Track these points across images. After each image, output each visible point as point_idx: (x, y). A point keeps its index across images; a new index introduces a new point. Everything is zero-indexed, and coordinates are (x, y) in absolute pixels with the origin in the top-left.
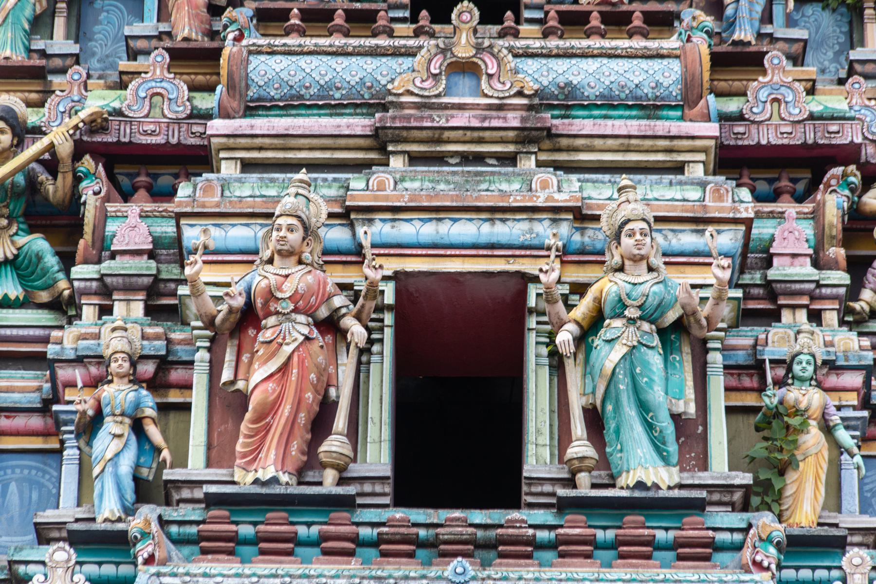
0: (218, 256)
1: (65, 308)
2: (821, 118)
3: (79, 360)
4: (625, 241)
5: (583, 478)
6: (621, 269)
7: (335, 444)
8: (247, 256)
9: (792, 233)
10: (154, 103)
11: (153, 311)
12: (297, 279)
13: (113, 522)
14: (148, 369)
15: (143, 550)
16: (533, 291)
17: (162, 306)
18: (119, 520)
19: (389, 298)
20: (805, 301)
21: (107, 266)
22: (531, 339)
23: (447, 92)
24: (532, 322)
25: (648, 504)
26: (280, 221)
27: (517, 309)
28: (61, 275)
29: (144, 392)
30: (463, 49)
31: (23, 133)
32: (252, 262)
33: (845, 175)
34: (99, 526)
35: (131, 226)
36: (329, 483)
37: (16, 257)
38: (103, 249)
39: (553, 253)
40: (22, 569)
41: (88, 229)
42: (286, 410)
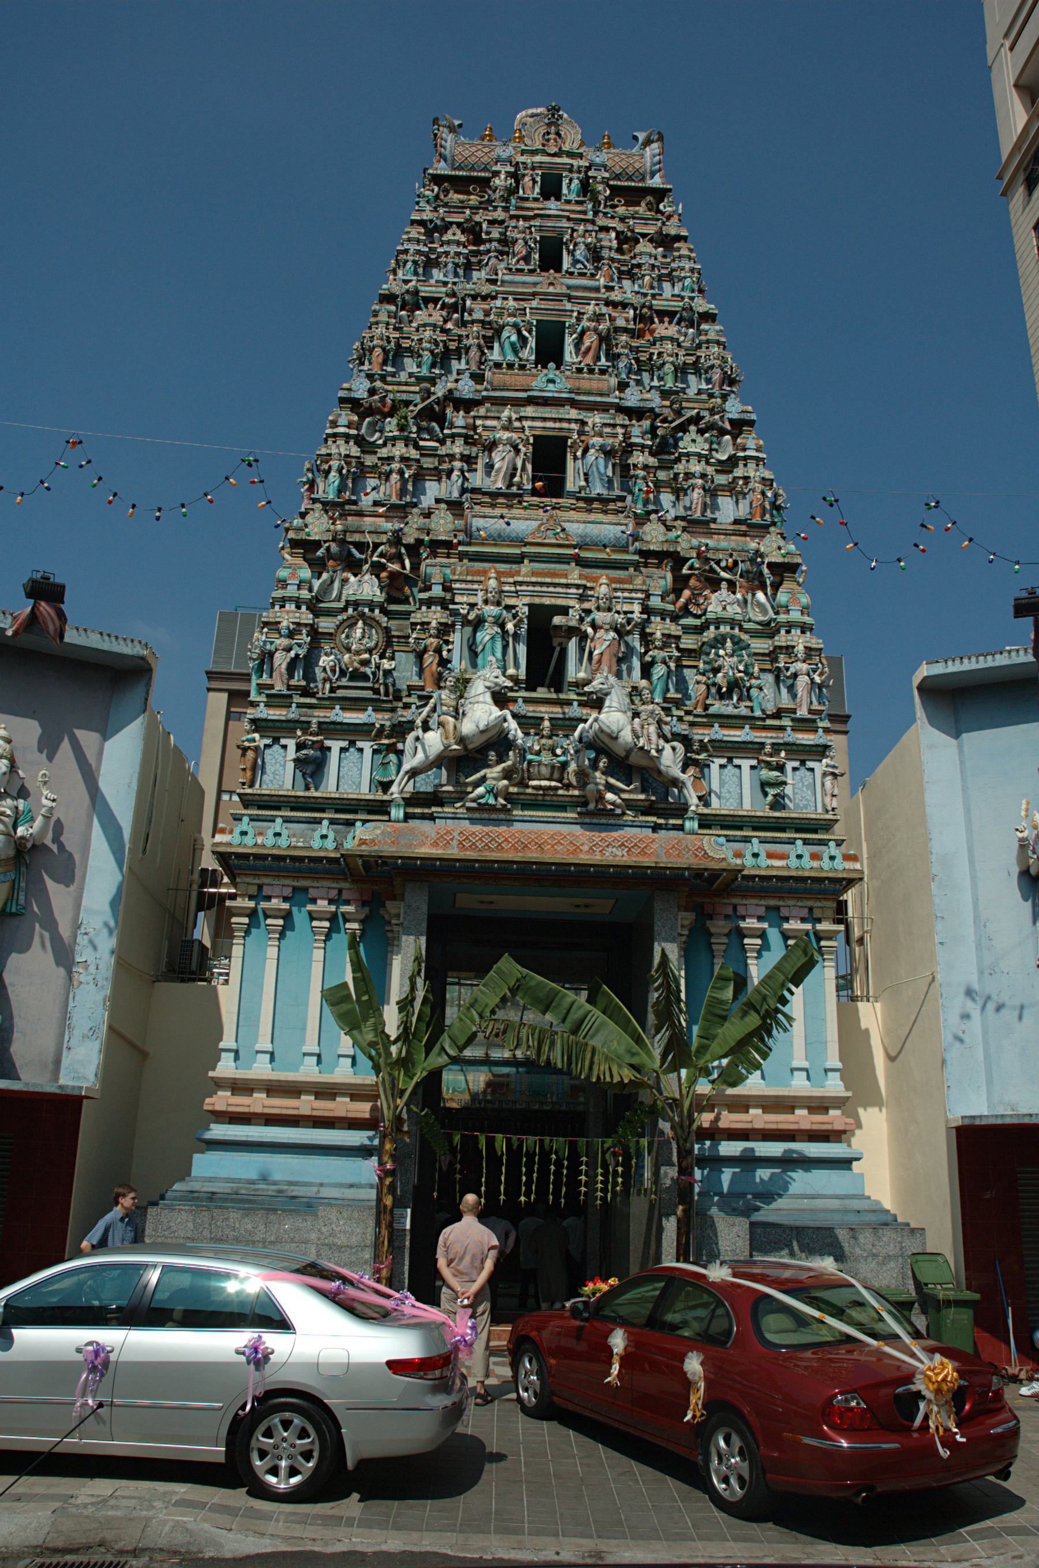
0: (485, 428)
1: (442, 442)
3: (447, 455)
7: (517, 479)
8: (493, 429)
9: (638, 431)
10: (466, 388)
11: (466, 443)
12: (506, 435)
15: (466, 505)
16: (570, 442)
17: (468, 441)
19: (531, 440)
25: (600, 499)
27: (565, 446)
30: (551, 376)
31: (429, 394)
35: (460, 419)
36: (514, 489)
38: (452, 426)
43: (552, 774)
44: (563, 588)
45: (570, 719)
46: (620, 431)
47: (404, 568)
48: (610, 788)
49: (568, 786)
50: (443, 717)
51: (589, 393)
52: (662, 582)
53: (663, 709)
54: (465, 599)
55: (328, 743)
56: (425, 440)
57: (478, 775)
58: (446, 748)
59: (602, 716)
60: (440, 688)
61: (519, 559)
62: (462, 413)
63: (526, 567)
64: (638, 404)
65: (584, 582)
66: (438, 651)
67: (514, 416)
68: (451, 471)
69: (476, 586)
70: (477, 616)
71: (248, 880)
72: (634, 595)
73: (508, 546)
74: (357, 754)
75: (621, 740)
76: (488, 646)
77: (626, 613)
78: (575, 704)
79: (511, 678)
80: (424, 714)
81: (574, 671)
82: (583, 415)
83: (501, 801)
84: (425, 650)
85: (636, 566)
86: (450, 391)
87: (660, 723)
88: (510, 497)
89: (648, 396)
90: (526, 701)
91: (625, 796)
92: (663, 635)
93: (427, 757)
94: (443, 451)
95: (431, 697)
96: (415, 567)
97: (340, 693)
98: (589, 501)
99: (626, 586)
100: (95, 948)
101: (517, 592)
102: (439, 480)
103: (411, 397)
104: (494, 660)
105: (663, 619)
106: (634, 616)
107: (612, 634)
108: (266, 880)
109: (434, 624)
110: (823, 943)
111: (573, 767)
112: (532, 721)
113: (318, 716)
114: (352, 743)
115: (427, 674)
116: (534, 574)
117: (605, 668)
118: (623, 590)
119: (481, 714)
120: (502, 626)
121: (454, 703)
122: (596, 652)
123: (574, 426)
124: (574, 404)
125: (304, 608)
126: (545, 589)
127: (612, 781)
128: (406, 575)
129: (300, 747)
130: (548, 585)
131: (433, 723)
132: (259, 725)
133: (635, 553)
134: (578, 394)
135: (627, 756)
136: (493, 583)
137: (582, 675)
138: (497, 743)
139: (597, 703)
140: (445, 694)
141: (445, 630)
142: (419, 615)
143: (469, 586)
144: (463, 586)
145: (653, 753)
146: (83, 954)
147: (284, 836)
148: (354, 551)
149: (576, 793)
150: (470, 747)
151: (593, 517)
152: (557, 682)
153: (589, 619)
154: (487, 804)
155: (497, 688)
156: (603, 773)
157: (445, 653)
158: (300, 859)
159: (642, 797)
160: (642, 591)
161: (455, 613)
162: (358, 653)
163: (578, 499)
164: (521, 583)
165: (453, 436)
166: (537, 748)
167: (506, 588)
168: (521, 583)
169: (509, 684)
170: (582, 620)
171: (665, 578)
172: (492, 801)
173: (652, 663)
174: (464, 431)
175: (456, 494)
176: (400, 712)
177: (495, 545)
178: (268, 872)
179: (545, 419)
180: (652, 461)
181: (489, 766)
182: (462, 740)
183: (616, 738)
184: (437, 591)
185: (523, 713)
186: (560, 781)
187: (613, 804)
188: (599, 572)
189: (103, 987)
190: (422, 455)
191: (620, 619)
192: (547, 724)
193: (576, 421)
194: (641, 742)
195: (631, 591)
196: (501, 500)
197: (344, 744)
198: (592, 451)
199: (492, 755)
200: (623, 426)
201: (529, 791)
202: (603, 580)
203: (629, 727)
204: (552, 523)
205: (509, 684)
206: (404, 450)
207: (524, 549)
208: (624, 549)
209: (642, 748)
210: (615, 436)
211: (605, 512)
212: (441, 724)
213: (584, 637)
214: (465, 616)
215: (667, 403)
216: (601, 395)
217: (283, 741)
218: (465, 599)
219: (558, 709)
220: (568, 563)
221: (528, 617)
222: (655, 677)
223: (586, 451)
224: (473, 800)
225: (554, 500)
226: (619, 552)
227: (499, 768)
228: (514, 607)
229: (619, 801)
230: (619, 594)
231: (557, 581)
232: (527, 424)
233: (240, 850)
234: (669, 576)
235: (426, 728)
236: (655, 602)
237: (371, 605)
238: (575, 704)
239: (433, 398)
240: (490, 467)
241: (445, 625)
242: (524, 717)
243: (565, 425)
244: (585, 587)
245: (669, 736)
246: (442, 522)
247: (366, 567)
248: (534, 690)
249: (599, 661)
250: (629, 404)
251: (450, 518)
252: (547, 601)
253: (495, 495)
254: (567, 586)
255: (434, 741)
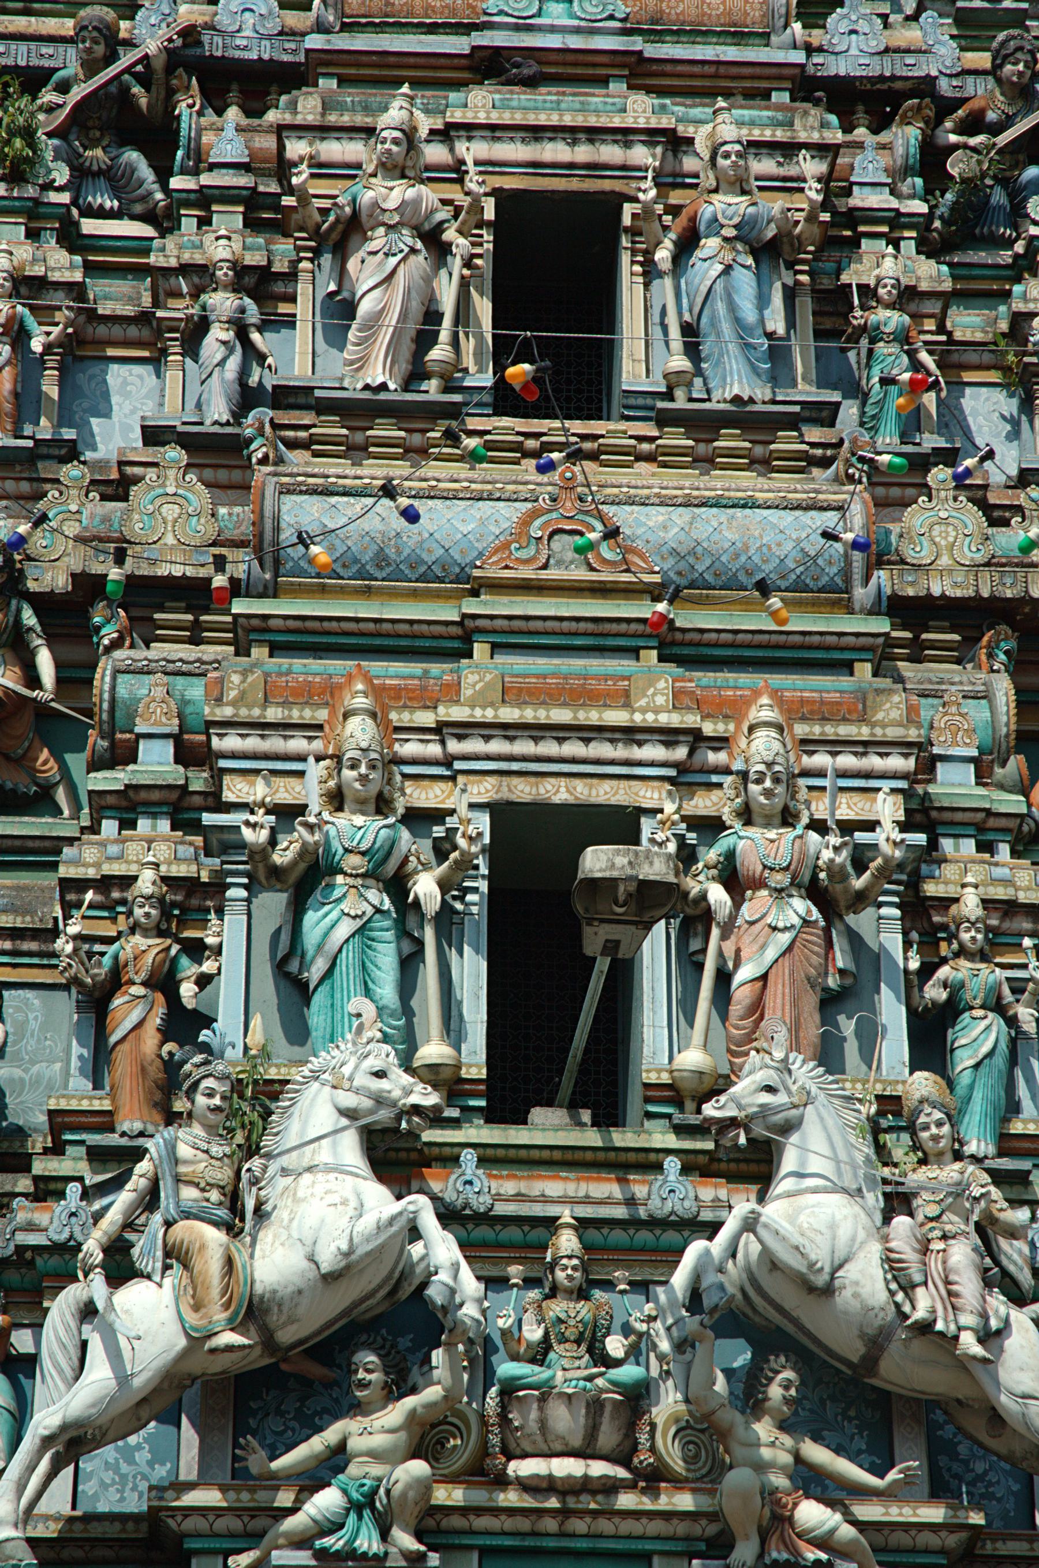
0: (322, 169)
2: (897, 50)
3: (184, 269)
4: (721, 162)
5: (680, 393)
6: (716, 191)
11: (252, 224)
12: (396, 194)
13: (221, 425)
14: (249, 280)
16: (628, 210)
17: (261, 215)
18: (228, 423)
19: (489, 214)
20: (885, 229)
21: (206, 179)
22: (625, 258)
23: (539, 14)
24: (625, 242)
25: (742, 417)
26: (384, 134)
28: (156, 186)
29: (247, 301)
31: (114, 45)
32: (354, 177)
33: (919, 108)
34: (208, 428)
35: (227, 138)
37: (110, 168)
38: (199, 162)
39: (650, 174)
40: (129, 470)
41: (183, 141)
42: (393, 318)
43: (592, 1432)
44: (611, 740)
45: (654, 1223)
46: (811, 167)
47: (33, 680)
48: (813, 1482)
49: (653, 1478)
50: (183, 1229)
51: (697, 34)
52: (978, 712)
53: (998, 1177)
54: (258, 790)
56: (102, 214)
57: (316, 1444)
58: (196, 1341)
59: (773, 1211)
60: (171, 1118)
61: (455, 643)
62: (233, 113)
63: (481, 670)
64: (876, 68)
65: (692, 720)
66: (164, 981)
67: (425, 124)
68: (200, 327)
69: (297, 744)
70: (305, 851)
72: (874, 762)
73: (414, 594)
75: (844, 1298)
76: (348, 959)
77: (847, 827)
78: (672, 1165)
79: (431, 1075)
80: (114, 1217)
81: (666, 1044)
82: (671, 113)
83: (405, 1540)
84: (116, 981)
85: (883, 656)
86: (190, 34)
87: (987, 1232)
88: (415, 418)
89: (911, 35)
90: (491, 1158)
91: (869, 1511)
92: (987, 903)
93: (123, 1379)
94: (168, 253)
95: (139, 1154)
96: (75, 678)
98: (703, 424)
99: (845, 731)
101: (448, 761)
102: (157, 361)
103: (44, 56)
104: (369, 1010)
105: (986, 847)
106: (879, 837)
107: (800, 906)
109: (146, 883)
111: (668, 1403)
112: (513, 1234)
115: (123, 1065)
116: (508, 694)
117: (776, 1027)
118: (835, 746)
119: (325, 1211)
120: (397, 885)
121: (224, 1174)
122: (745, 973)
123: (641, 155)
124: (641, 73)
126: (549, 748)
127: (818, 1453)
128: (42, 711)
130: (561, 732)
131: (146, 1249)
133: (873, 611)
134: (655, 35)
135: (871, 1360)
136: (359, 731)
137: (693, 1058)
138: (386, 1320)
139: (754, 1161)
140: (189, 1143)
141: (186, 905)
142: (90, 854)
143: (275, 743)
144: (253, 743)
145: (969, 1343)
149: (685, 1501)
150: (286, 1336)
151: (719, 482)
152: (603, 1086)
153: (712, 855)
154: (350, 1554)
155: (384, 1115)
156: (783, 1426)
157: (187, 990)
159: (934, 1513)
160: (905, 746)
161: (223, 843)
163: (664, 419)
164: (463, 729)
165: (205, 200)
166: (533, 1333)
167: (411, 748)
168: (463, 729)
169: (427, 1097)
170: (687, 856)
171: (986, 696)
172: (368, 1542)
173: (951, 1010)
174: (244, 180)
175: (218, 410)
176: (23, 1211)
177: (367, 592)
179: (536, 133)
180: (930, 274)
181: (358, 1408)
182: (253, 1312)
183: (828, 1291)
184: (156, 763)
185: (480, 1203)
186: (626, 1464)
187: (823, 1542)
188: (745, 679)
190: (89, 268)
191: (827, 850)
192: (567, 1242)
193: (652, 136)
194: (924, 1304)
195: (865, 747)
196: (384, 430)
198: (710, 244)
199: (369, 1367)
200: (822, 150)
201: (510, 1498)
202: (764, 711)
203: (875, 1249)
204: (569, 507)
205: (427, 1097)
206: (25, 252)
207: (471, 606)
208: (836, 596)
209: (925, 1328)
210: (792, 186)
211: (764, 465)
212: (176, 1255)
213: (696, 919)
214: (260, 855)
215: (982, 59)
216: (739, 37)
218: (258, 790)
219: (607, 1188)
220: (634, 652)
221: (492, 852)
222: (964, 1061)
223: (688, 243)
224: (301, 1542)
225: (577, 426)
226: (814, 606)
227: (395, 1413)
228: (438, 816)
229: (847, 1531)
230: (821, 760)
231: (593, 717)
232: (471, 151)
234: (1003, 688)
235: (120, 1268)
236: (955, 784)
238: (672, 1165)
239: (127, 58)
240: (340, 310)
241: (189, 885)
242: (486, 1218)
243: (610, 153)
244: (696, 738)
245: (1025, 1278)
246: (170, 511)
248: (521, 1119)
249: (757, 1008)
250: (839, 67)
251: (199, 496)
252: (559, 792)
253: (360, 411)
254: (631, 734)
255: (150, 1318)
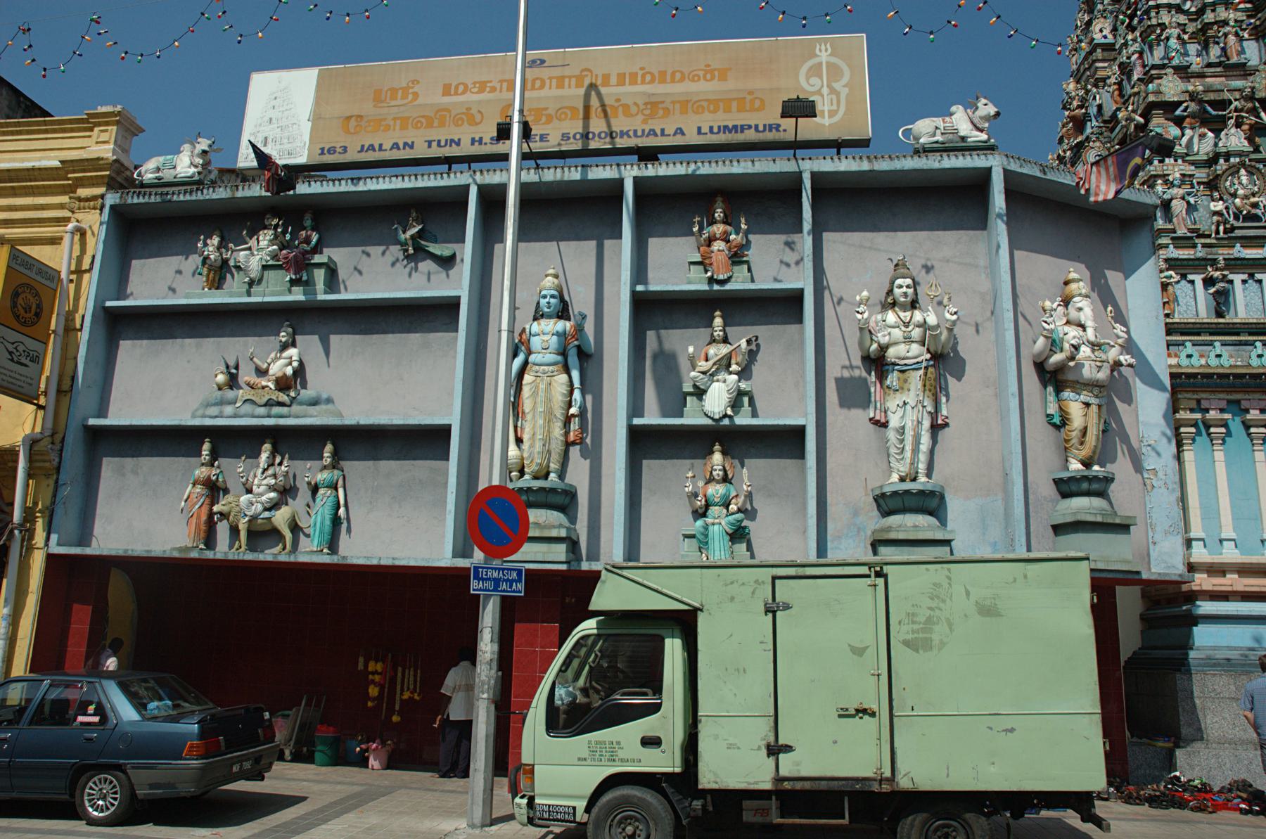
55: (1231, 277)
71: (1189, 395)
74: (1256, 286)
97: (1238, 233)
100: (1158, 454)
108: (1204, 395)
110: (1212, 430)
113: (1222, 254)
114: (1251, 276)
125: (1180, 161)
129: (1209, 282)
132: (1172, 264)
146: (1150, 462)
147: (1225, 355)
148: (1209, 109)
158: (1243, 376)
162: (1246, 197)
178: (1246, 389)
189: (1174, 490)
197: (1245, 277)
217: (1190, 277)
233: (1190, 371)
237: (1240, 154)
247: (1232, 121)
